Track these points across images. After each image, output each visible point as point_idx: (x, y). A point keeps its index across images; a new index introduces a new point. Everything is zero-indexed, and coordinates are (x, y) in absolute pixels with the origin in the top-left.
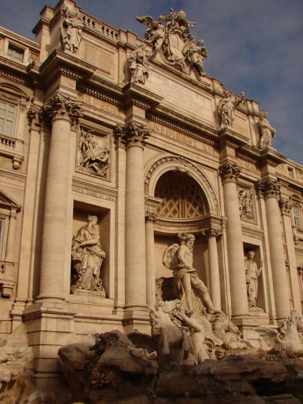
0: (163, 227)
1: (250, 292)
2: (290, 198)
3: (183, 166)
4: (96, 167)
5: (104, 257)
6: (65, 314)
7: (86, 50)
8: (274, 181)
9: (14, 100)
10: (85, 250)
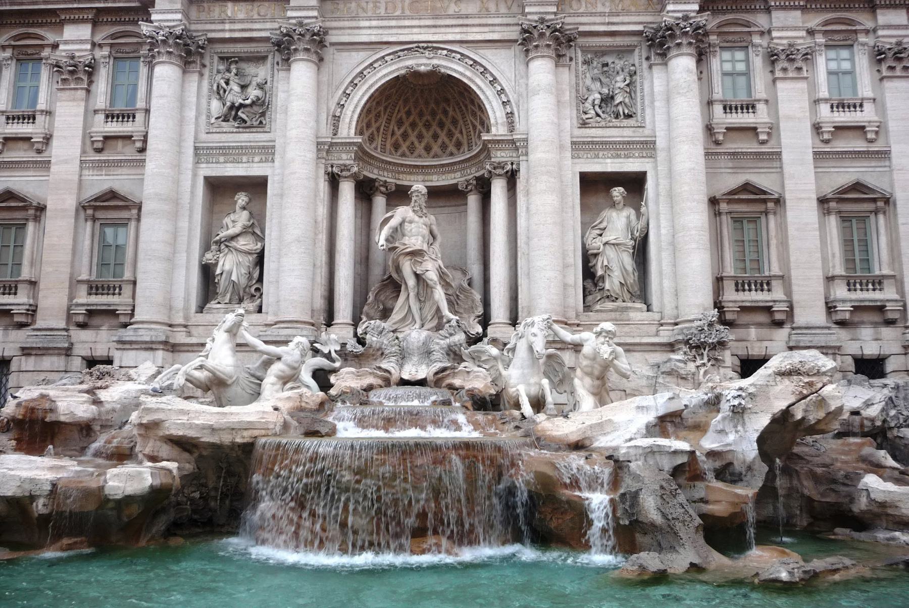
0: (435, 177)
1: (600, 272)
2: (811, 32)
3: (424, 61)
4: (244, 116)
6: (146, 342)
8: (680, 15)
9: (133, 52)
10: (223, 247)
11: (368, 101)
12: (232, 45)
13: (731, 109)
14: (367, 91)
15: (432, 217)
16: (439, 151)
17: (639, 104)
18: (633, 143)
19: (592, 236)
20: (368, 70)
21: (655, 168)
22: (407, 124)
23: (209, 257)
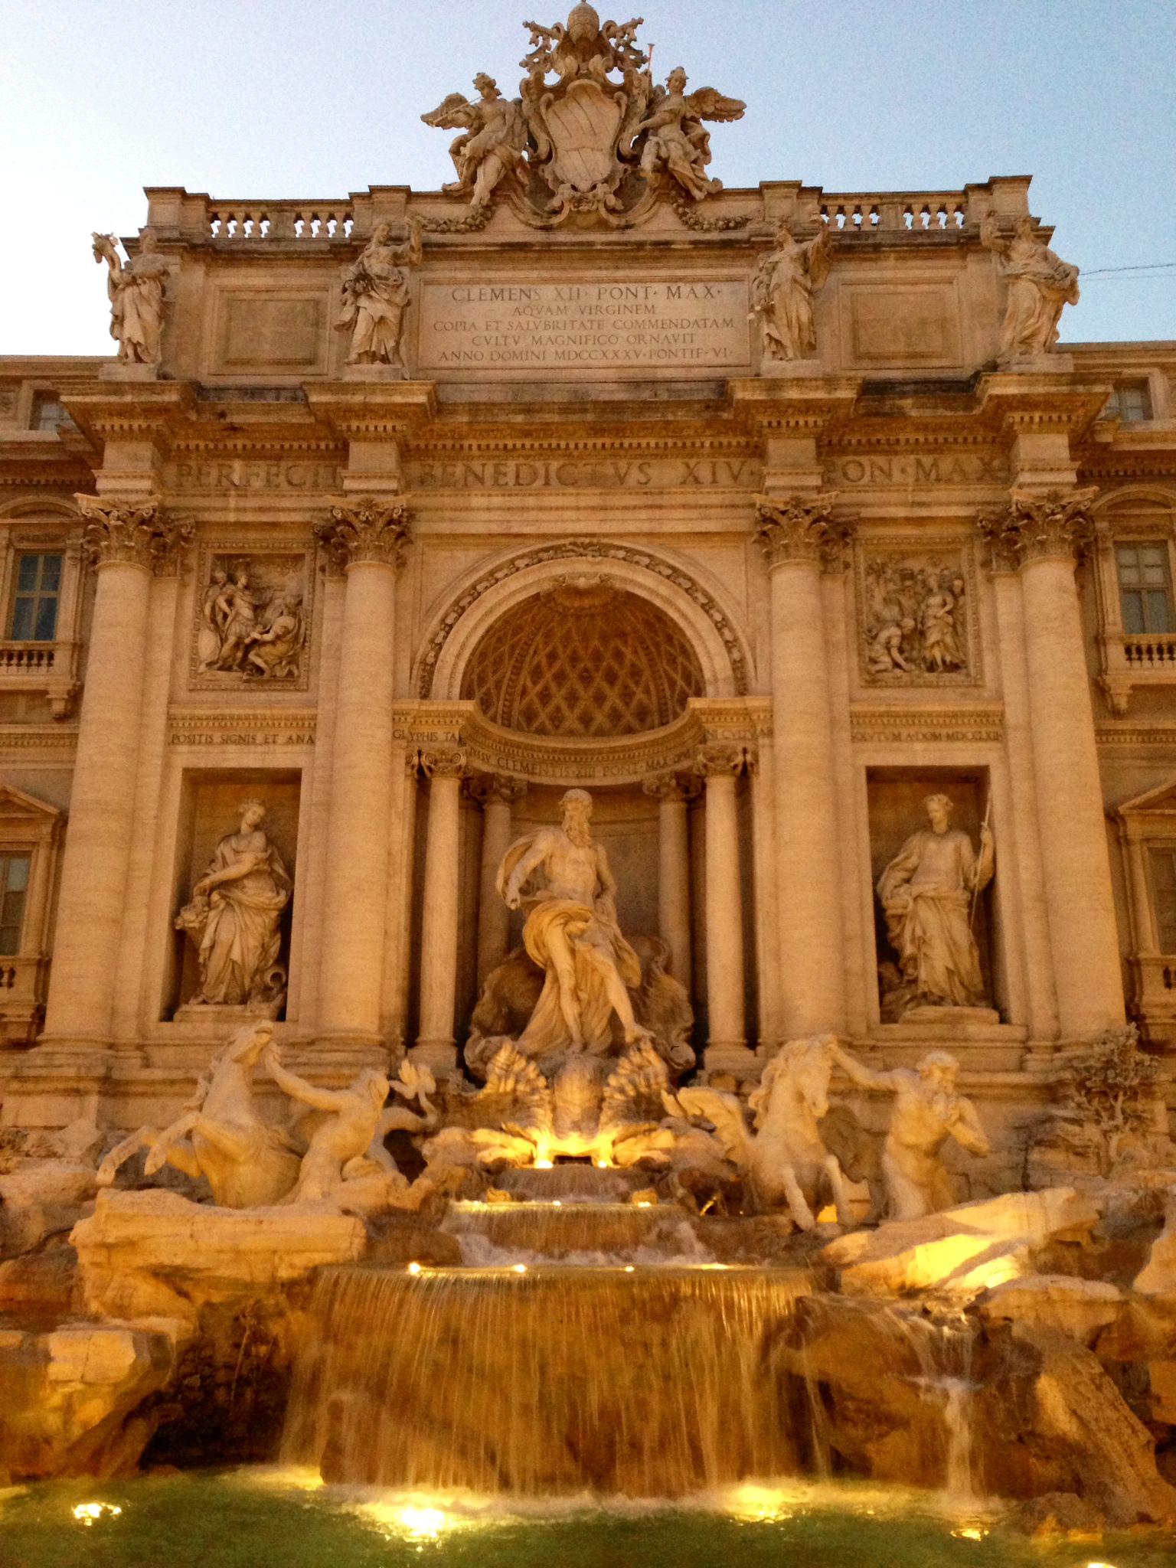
0: (599, 771)
1: (909, 950)
4: (259, 662)
5: (281, 905)
6: (68, 1079)
7: (230, 319)
8: (1045, 490)
10: (215, 897)
11: (483, 637)
12: (240, 535)
13: (1139, 650)
14: (481, 620)
15: (601, 850)
16: (606, 724)
17: (971, 643)
18: (963, 714)
19: (893, 882)
20: (485, 584)
21: (1005, 759)
22: (548, 676)
23: (189, 918)
